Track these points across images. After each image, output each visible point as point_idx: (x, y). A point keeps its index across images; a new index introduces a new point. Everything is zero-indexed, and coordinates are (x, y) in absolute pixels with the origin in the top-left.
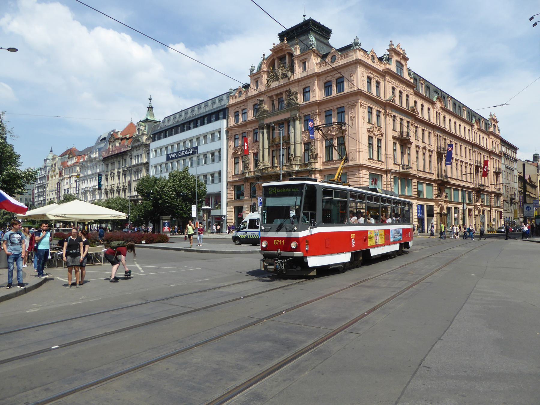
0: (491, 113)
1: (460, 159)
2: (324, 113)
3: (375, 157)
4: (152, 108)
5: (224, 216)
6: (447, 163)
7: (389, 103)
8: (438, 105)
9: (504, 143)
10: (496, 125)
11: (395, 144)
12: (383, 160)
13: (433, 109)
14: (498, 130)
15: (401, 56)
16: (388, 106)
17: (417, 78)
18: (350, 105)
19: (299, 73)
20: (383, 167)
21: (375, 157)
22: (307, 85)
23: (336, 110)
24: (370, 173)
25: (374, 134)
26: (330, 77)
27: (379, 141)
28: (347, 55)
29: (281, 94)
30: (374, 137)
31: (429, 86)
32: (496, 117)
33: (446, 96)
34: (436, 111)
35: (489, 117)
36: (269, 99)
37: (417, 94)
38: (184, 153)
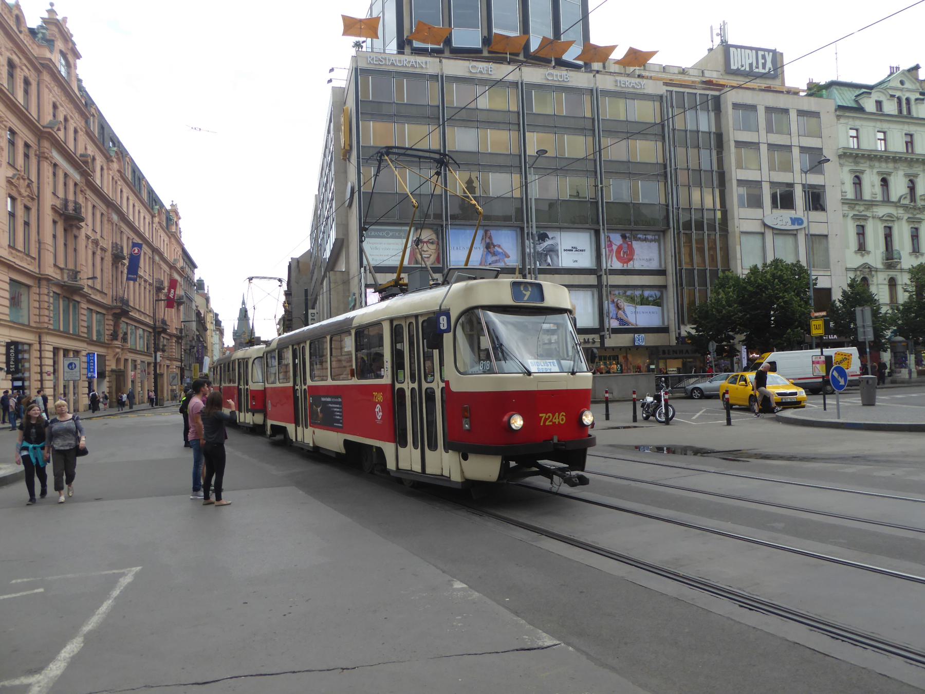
0: (172, 201)
3: (20, 245)
6: (130, 276)
7: (50, 134)
8: (115, 166)
9: (186, 255)
11: (55, 222)
12: (34, 253)
13: (108, 171)
16: (47, 139)
20: (32, 268)
21: (20, 245)
25: (20, 194)
27: (27, 208)
30: (19, 199)
34: (112, 174)
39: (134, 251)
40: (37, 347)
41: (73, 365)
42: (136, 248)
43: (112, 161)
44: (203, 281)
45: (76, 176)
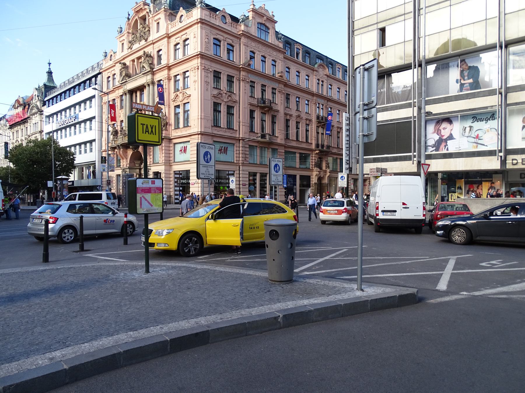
5: (100, 186)
15: (265, 18)
17: (289, 42)
19: (153, 36)
26: (179, 39)
31: (308, 51)
33: (334, 63)
40: (238, 172)
42: (330, 116)
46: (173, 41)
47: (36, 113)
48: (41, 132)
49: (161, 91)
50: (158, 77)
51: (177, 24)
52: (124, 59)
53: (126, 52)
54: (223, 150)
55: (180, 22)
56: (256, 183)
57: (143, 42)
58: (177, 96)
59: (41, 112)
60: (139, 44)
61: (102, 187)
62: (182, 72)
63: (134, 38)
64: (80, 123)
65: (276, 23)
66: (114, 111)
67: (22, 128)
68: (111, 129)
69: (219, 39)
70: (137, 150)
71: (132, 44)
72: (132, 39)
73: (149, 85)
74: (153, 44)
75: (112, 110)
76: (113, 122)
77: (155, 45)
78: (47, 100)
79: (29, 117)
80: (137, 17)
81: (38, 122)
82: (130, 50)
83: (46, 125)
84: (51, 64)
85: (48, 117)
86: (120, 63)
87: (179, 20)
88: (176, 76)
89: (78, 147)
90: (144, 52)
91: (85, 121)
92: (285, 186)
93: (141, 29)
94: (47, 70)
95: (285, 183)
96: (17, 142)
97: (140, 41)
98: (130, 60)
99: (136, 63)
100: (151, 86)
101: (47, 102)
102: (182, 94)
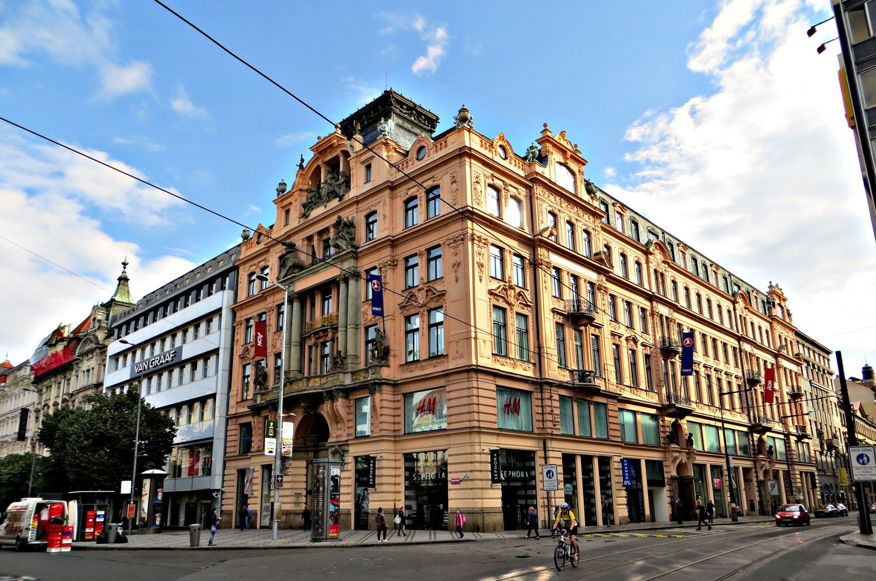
0: (770, 282)
1: (715, 366)
2: (404, 261)
4: (126, 279)
5: (218, 490)
6: (684, 370)
10: (783, 304)
14: (789, 315)
16: (541, 247)
18: (452, 241)
19: (358, 188)
22: (373, 209)
23: (426, 254)
24: (497, 386)
28: (446, 142)
29: (327, 230)
32: (781, 289)
35: (768, 290)
36: (306, 242)
37: (608, 230)
38: (159, 362)
39: (686, 341)
40: (541, 454)
41: (551, 473)
43: (651, 254)
44: (870, 368)
45: (593, 276)
46: (402, 193)
47: (91, 351)
48: (99, 385)
49: (377, 289)
50: (365, 263)
51: (410, 163)
52: (289, 237)
53: (295, 222)
54: (512, 406)
55: (417, 159)
56: (575, 479)
57: (335, 203)
58: (412, 296)
59: (103, 349)
60: (325, 207)
61: (223, 492)
62: (423, 249)
63: (313, 199)
64: (182, 364)
65: (585, 164)
66: (262, 336)
67: (59, 381)
68: (249, 371)
69: (497, 185)
70: (315, 412)
71: (308, 210)
72: (310, 201)
73: (346, 281)
74: (357, 204)
75: (259, 333)
76: (257, 358)
77: (360, 205)
78: (116, 327)
79: (77, 359)
80: (320, 162)
81: (93, 368)
82: (302, 221)
83: (109, 372)
84: (127, 264)
85: (116, 357)
86: (284, 244)
87: (415, 156)
88: (407, 259)
89: (185, 409)
90: (339, 217)
91: (193, 361)
92: (627, 483)
93: (328, 180)
94: (120, 274)
95: (627, 478)
96: (46, 408)
97: (328, 202)
98: (302, 237)
99: (315, 242)
100: (352, 283)
101: (116, 331)
102: (424, 292)
